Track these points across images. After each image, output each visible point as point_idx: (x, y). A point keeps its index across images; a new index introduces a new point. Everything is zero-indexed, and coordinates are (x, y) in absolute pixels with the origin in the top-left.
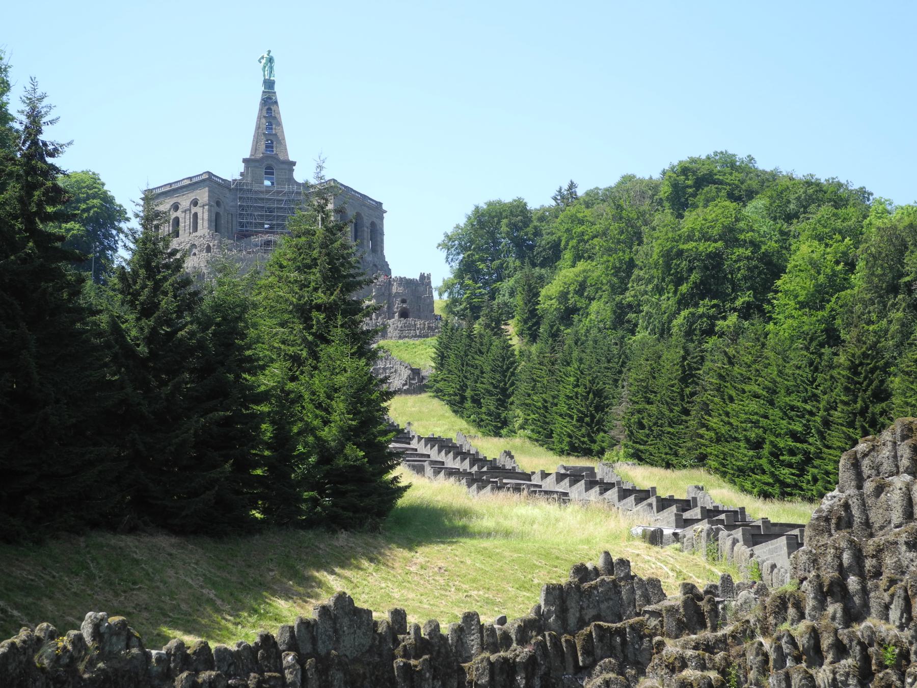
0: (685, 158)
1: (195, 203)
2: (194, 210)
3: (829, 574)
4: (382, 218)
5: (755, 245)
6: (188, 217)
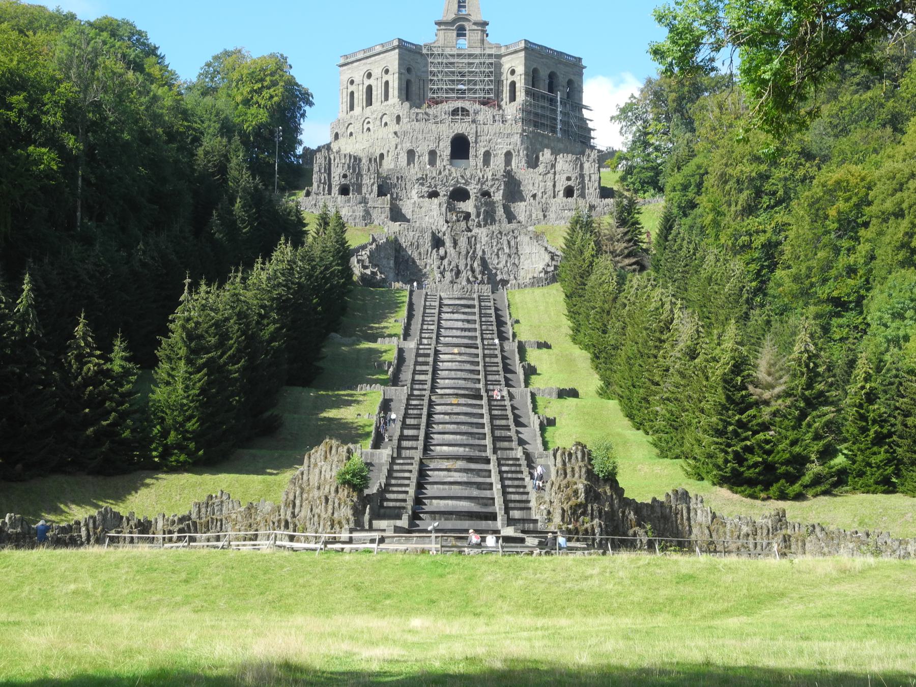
2: (385, 78)
4: (581, 75)
6: (379, 85)
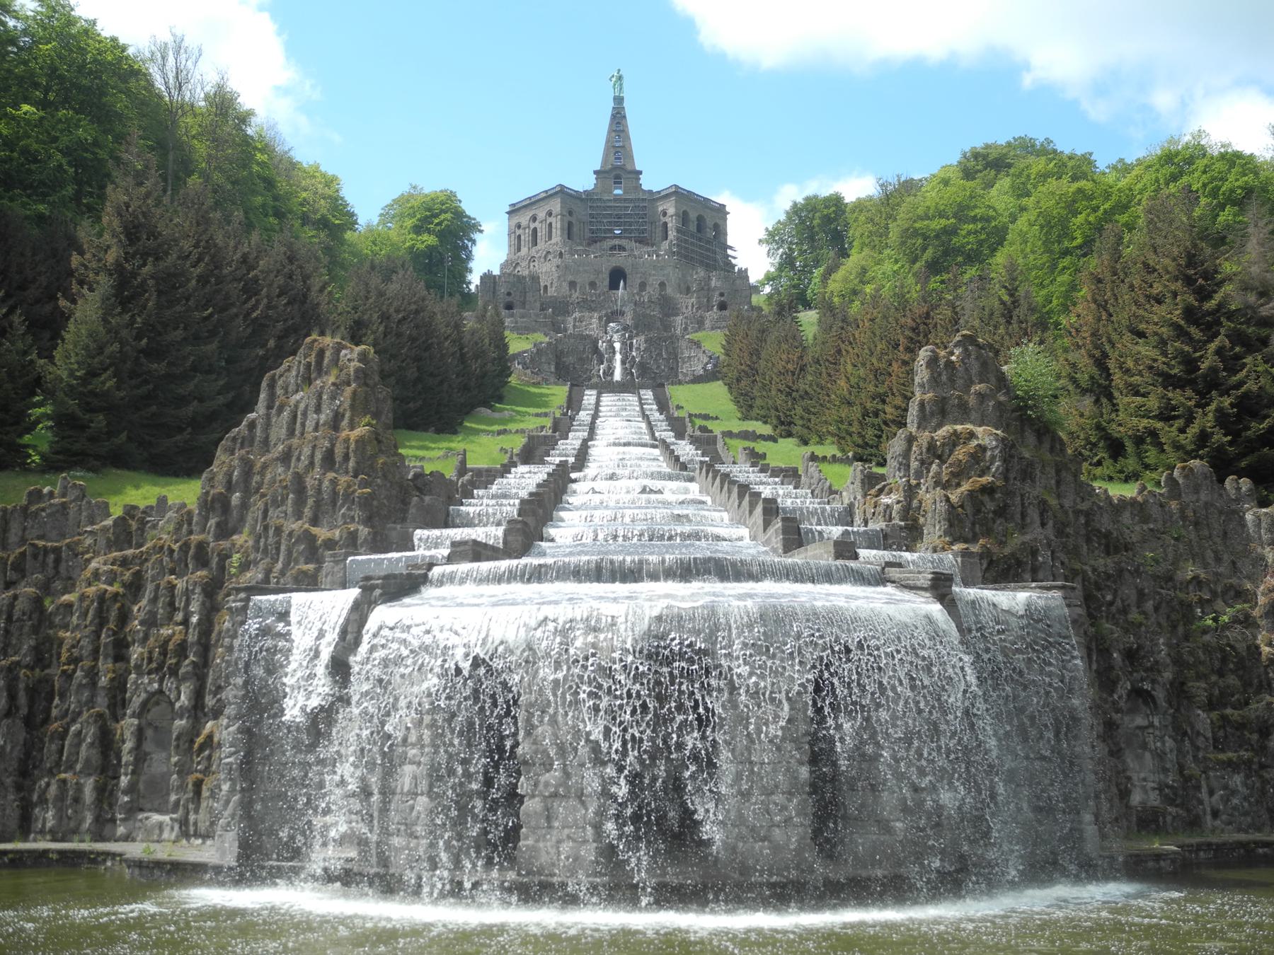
0: (978, 143)
1: (550, 214)
3: (220, 489)
4: (725, 220)
5: (987, 219)
